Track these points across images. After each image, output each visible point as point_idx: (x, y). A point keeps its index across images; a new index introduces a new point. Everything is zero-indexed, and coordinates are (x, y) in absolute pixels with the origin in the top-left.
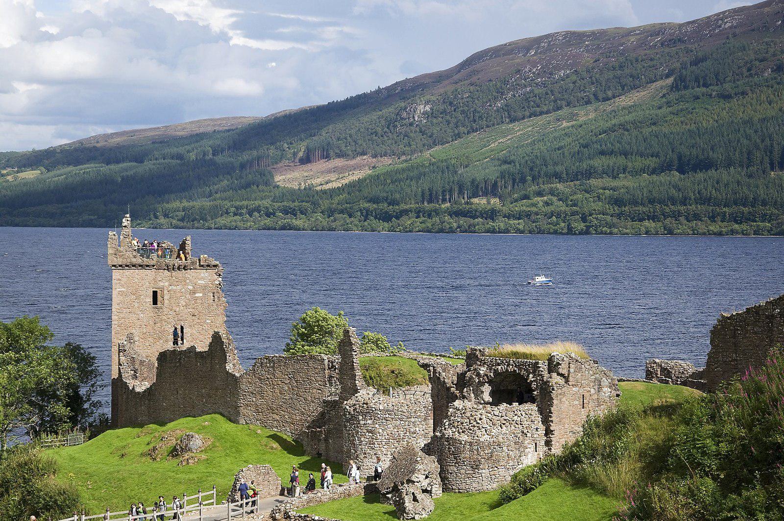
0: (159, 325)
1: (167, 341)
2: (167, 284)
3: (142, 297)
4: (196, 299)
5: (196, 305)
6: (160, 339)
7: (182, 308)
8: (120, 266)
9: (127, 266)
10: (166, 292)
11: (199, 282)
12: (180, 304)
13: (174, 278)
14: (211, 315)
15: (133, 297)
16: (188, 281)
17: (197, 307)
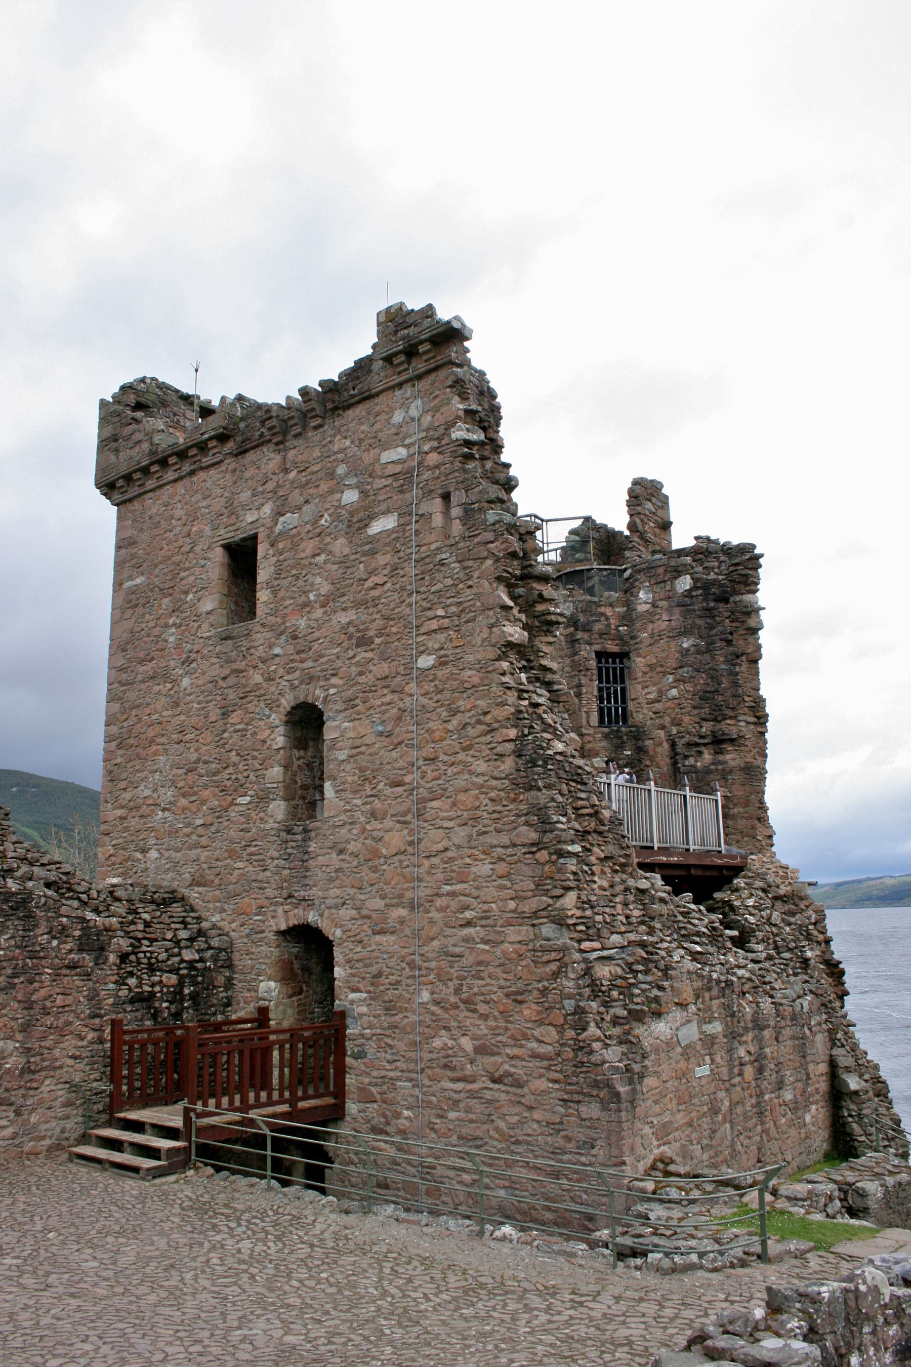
0: (235, 718)
1: (263, 798)
2: (267, 510)
3: (190, 596)
4: (373, 546)
5: (369, 584)
6: (240, 788)
7: (319, 613)
8: (128, 478)
9: (145, 471)
10: (261, 550)
11: (386, 457)
12: (312, 597)
13: (293, 475)
14: (434, 624)
15: (166, 601)
16: (341, 470)
17: (375, 593)
